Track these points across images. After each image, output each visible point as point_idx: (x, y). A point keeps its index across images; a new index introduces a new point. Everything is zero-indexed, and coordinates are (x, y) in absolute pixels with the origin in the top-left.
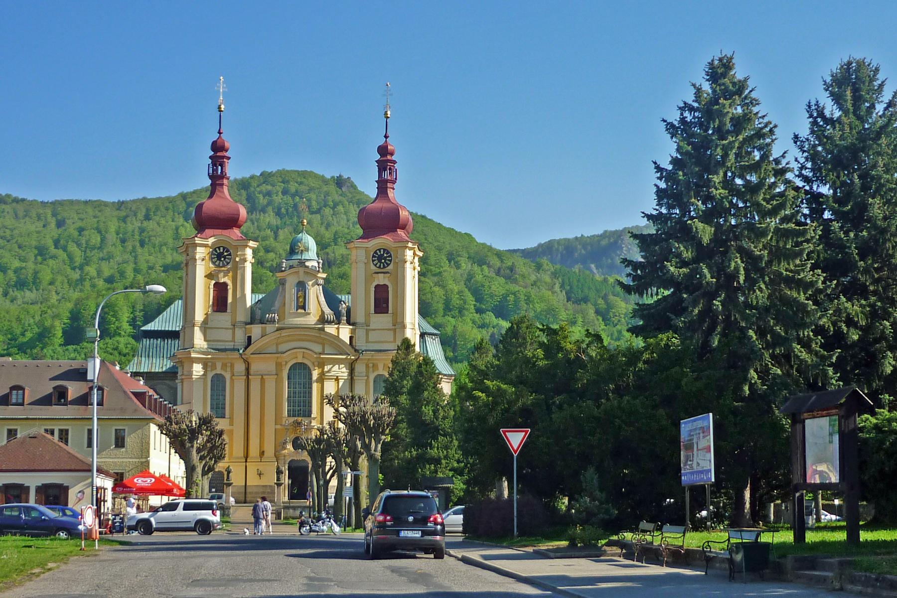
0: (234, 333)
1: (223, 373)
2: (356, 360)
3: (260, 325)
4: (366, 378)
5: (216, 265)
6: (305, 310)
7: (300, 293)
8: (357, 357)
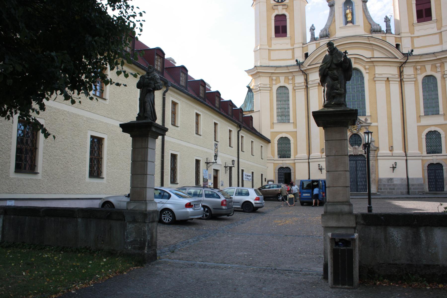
0: (293, 53)
1: (286, 85)
2: (405, 63)
3: (315, 42)
4: (415, 79)
5: (276, 2)
6: (353, 24)
7: (348, 11)
8: (404, 61)
